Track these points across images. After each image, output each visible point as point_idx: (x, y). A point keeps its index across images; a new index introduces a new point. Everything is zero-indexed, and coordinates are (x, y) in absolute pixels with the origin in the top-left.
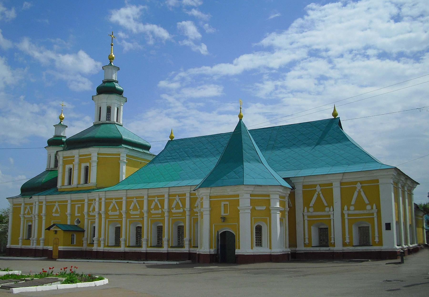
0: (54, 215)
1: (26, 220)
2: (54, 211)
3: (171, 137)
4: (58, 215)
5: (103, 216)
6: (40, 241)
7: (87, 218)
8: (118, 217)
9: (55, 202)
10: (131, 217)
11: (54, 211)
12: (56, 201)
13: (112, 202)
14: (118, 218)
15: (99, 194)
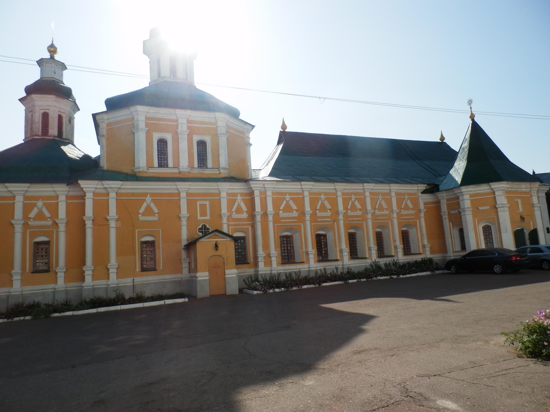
0: (141, 218)
1: (28, 234)
2: (142, 210)
3: (284, 126)
4: (155, 218)
5: (270, 218)
6: (84, 273)
7: (227, 224)
8: (296, 220)
9: (145, 195)
10: (319, 220)
11: (142, 210)
12: (148, 193)
13: (285, 198)
14: (330, 221)
15: (264, 185)
